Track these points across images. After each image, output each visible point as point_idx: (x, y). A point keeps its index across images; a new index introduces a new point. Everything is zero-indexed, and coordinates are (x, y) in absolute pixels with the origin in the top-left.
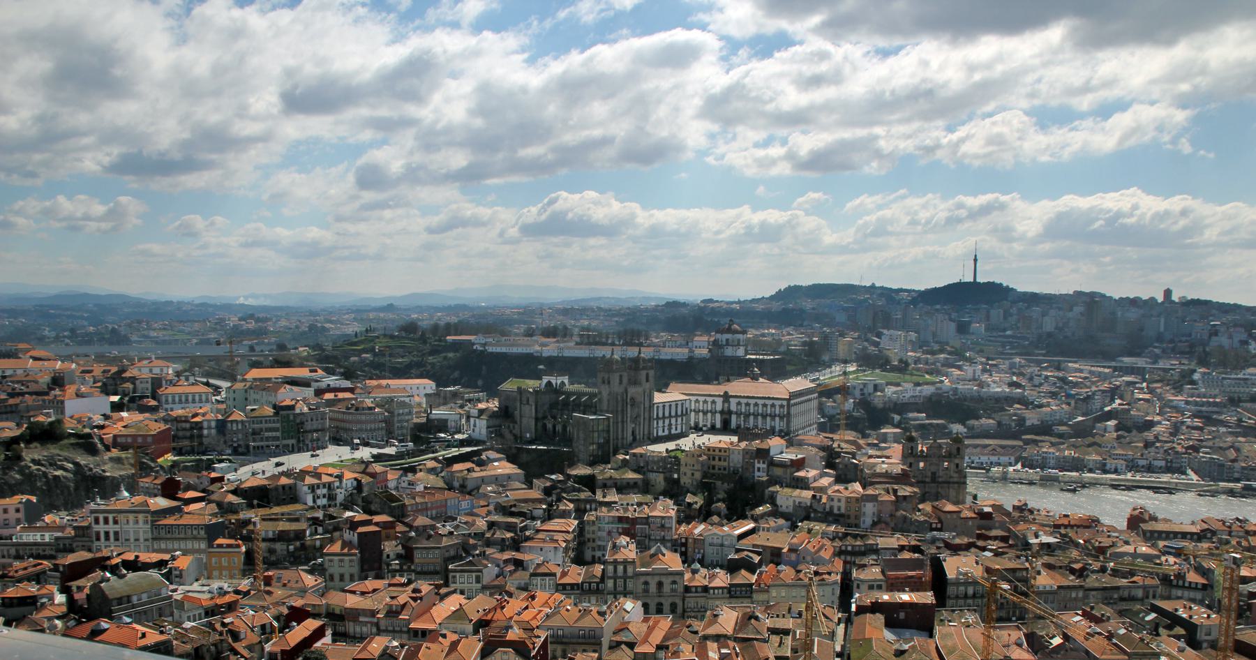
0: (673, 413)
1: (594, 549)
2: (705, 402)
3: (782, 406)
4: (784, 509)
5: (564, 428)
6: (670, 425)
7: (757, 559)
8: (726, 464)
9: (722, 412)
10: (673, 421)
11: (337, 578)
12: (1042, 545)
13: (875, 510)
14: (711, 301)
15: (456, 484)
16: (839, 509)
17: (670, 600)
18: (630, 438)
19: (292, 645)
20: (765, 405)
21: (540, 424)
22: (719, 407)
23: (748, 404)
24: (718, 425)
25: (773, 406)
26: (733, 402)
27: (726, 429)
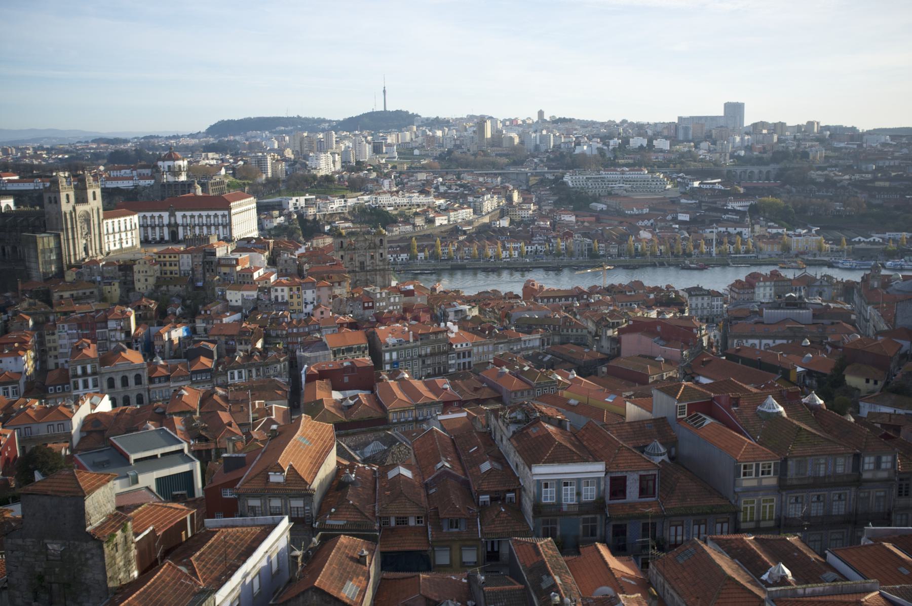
0: (123, 229)
1: (56, 357)
2: (152, 217)
3: (224, 216)
4: (234, 303)
5: (14, 249)
6: (121, 239)
7: (213, 347)
9: (169, 225)
10: (123, 235)
12: (456, 312)
13: (314, 295)
14: (151, 137)
16: (283, 296)
17: (135, 394)
20: (208, 216)
22: (166, 221)
23: (192, 217)
24: (167, 238)
25: (216, 216)
27: (174, 239)
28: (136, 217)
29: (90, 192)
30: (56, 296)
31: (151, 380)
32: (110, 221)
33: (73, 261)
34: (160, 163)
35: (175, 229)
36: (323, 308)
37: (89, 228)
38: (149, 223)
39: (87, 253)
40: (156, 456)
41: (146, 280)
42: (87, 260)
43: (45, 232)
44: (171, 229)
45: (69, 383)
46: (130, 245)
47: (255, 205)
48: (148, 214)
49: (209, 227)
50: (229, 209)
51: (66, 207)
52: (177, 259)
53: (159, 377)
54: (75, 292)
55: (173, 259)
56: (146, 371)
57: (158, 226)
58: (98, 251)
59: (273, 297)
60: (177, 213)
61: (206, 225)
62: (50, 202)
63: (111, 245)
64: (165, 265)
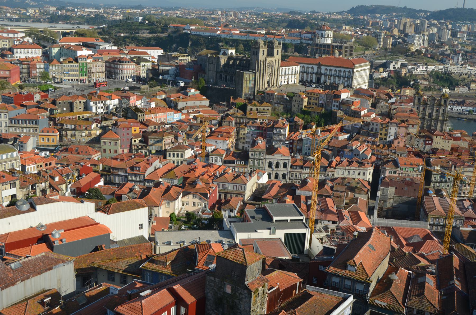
0: (290, 73)
2: (308, 67)
3: (349, 72)
6: (288, 79)
8: (317, 102)
9: (317, 74)
11: (107, 151)
13: (395, 131)
15: (172, 105)
16: (376, 129)
18: (266, 86)
19: (83, 185)
20: (340, 71)
21: (218, 75)
22: (315, 71)
23: (331, 70)
24: (314, 80)
25: (345, 71)
26: (323, 68)
28: (299, 67)
29: (275, 50)
30: (249, 108)
31: (292, 167)
32: (284, 68)
33: (261, 88)
34: (317, 31)
35: (319, 76)
36: (399, 140)
37: (272, 71)
38: (305, 71)
39: (269, 85)
40: (287, 220)
41: (299, 106)
42: (268, 89)
43: (248, 71)
44: (318, 76)
45: (248, 161)
46: (293, 82)
47: (369, 67)
48: (306, 66)
49: (339, 77)
50: (353, 68)
51: (262, 58)
52: (318, 96)
53: (297, 166)
54: (259, 108)
55: (315, 96)
56: (290, 161)
57: (311, 73)
58: (275, 85)
59: (370, 128)
60: (322, 67)
61: (338, 76)
62: (254, 54)
63: (283, 81)
64: (310, 99)
